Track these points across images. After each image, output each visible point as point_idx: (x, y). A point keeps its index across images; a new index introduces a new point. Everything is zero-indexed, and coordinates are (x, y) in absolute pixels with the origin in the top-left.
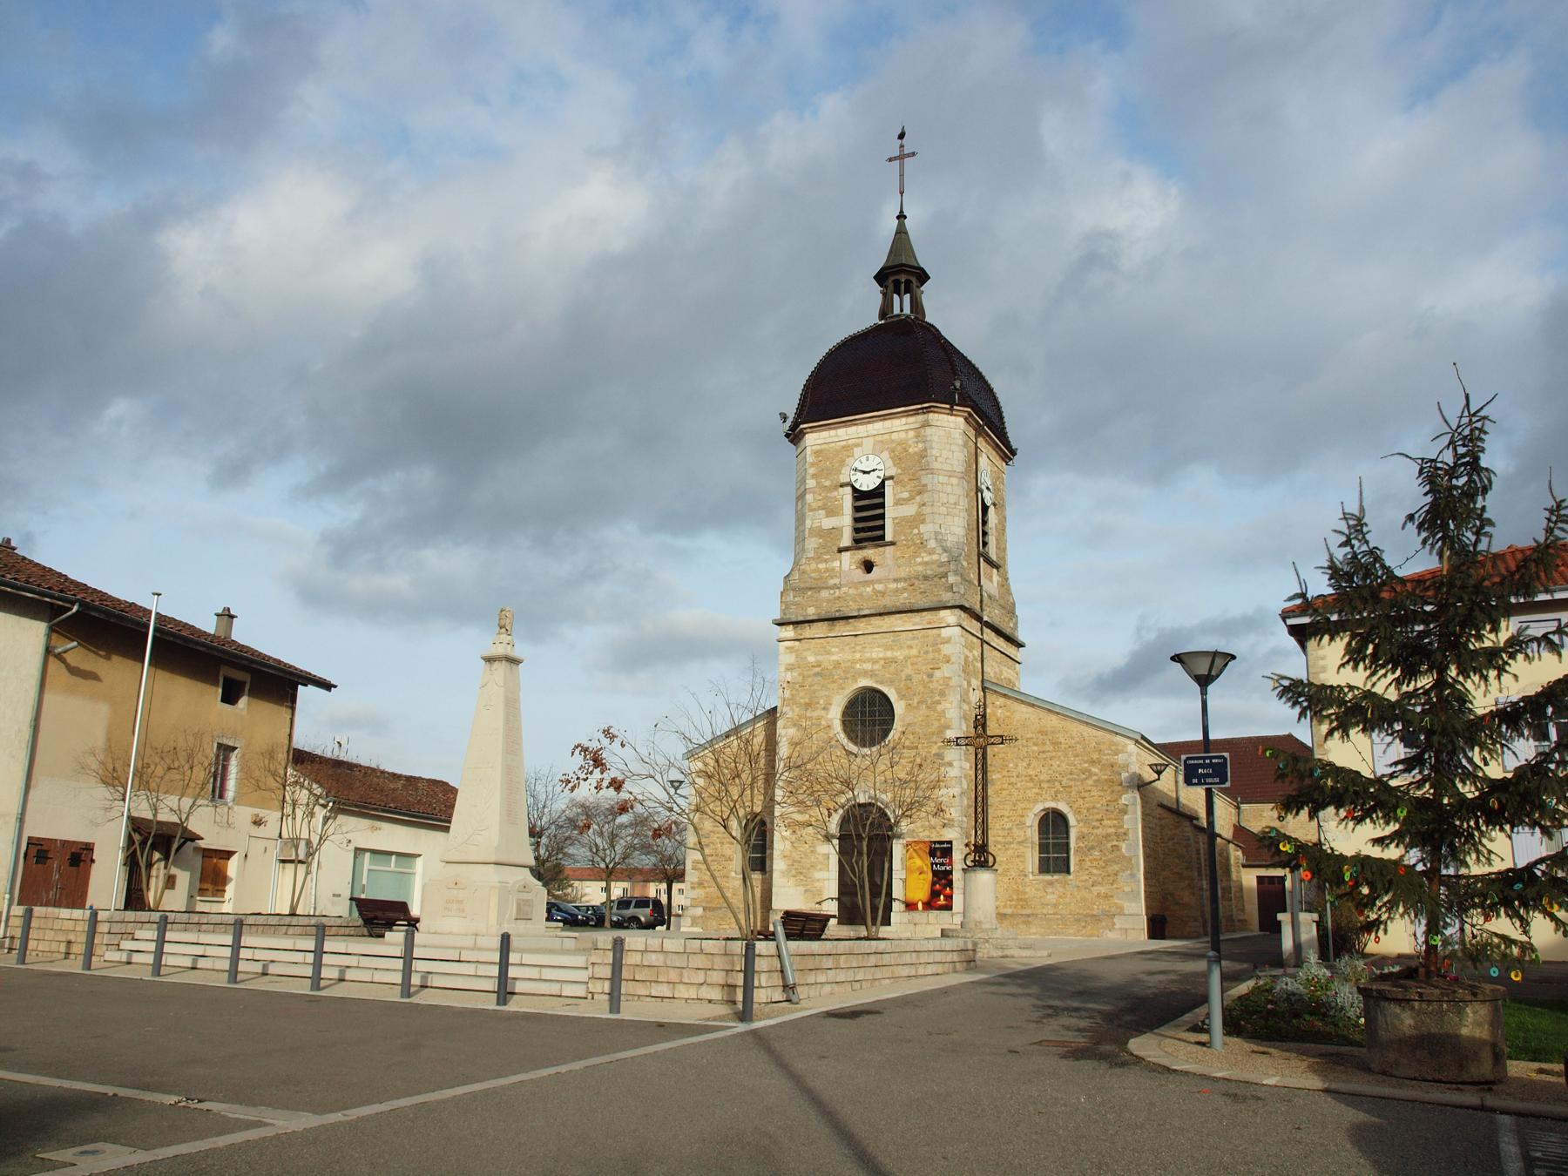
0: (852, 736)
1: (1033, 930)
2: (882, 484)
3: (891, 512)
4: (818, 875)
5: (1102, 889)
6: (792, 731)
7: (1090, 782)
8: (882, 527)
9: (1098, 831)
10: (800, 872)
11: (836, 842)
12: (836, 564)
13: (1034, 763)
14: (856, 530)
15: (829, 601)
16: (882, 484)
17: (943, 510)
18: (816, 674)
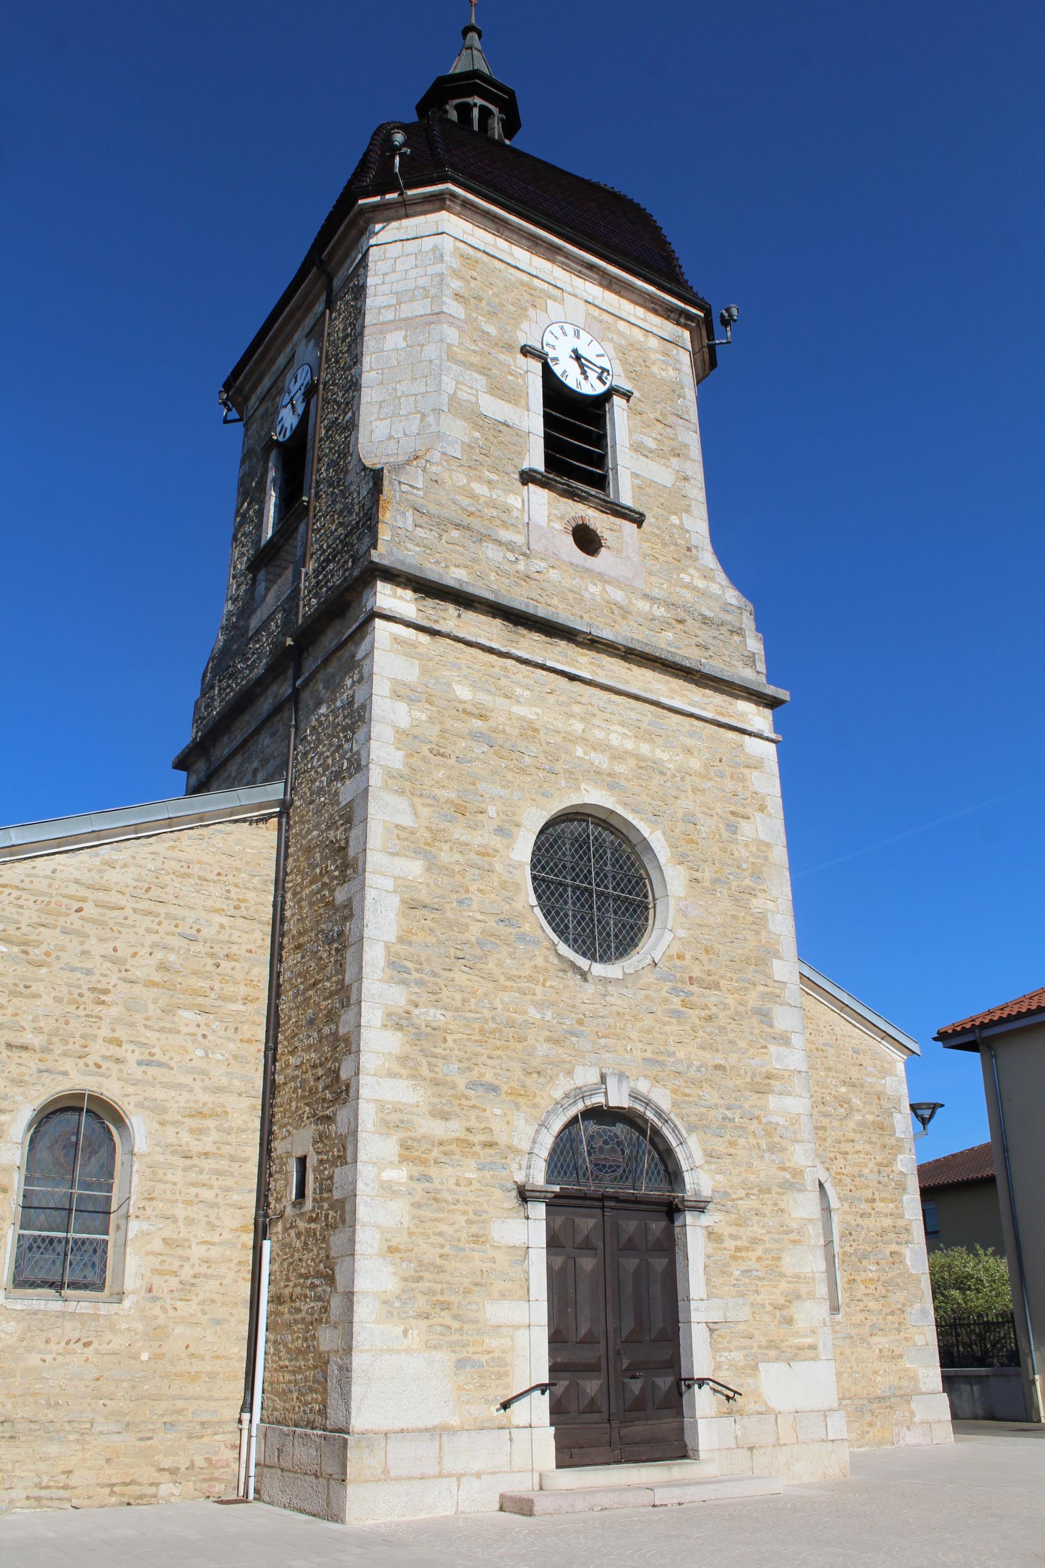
6: (414, 868)
7: (851, 1124)
10: (439, 1301)
11: (539, 1210)
15: (499, 571)
16: (606, 397)
18: (475, 736)
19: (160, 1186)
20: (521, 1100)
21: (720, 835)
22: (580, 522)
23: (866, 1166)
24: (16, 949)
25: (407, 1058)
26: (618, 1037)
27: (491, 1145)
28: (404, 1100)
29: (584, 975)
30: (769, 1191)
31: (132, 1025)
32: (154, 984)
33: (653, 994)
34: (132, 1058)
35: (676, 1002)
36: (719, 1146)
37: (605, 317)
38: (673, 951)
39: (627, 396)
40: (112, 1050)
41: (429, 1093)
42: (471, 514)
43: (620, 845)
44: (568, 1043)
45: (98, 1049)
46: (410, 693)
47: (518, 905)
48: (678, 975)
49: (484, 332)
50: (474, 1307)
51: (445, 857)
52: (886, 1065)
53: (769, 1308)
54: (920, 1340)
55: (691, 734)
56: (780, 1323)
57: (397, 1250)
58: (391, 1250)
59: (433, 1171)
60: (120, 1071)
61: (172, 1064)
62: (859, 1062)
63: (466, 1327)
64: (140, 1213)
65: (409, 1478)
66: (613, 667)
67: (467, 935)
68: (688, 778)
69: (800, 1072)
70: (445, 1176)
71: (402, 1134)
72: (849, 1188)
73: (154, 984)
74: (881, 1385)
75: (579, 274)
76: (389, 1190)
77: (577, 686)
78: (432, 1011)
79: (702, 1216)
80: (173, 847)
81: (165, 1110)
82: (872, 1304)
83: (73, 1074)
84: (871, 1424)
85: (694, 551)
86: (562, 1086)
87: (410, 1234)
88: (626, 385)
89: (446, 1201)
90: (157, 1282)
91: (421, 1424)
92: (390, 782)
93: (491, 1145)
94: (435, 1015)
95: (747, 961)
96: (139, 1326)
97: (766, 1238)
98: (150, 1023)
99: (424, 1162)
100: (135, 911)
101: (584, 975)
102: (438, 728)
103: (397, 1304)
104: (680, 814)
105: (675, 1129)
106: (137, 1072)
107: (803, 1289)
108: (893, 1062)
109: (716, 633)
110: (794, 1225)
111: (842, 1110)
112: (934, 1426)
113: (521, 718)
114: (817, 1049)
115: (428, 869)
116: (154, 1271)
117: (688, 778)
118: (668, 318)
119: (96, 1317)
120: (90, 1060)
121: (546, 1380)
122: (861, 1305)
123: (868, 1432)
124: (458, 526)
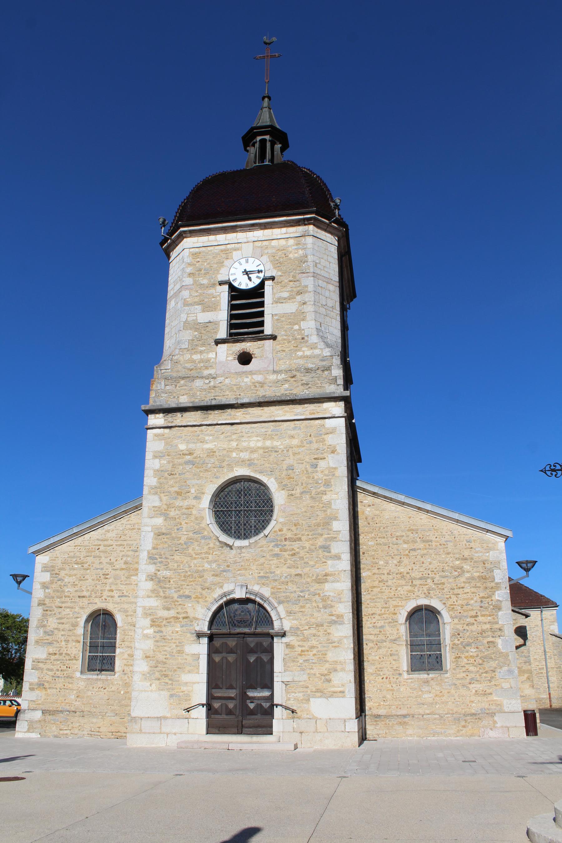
0: (225, 527)
1: (410, 731)
2: (262, 285)
3: (270, 309)
4: (185, 678)
5: (479, 687)
6: (159, 521)
8: (262, 324)
9: (474, 628)
11: (205, 640)
12: (212, 355)
13: (406, 561)
14: (232, 326)
15: (201, 390)
16: (262, 285)
17: (322, 310)
18: (187, 463)
19: (127, 637)
20: (200, 600)
21: (307, 471)
22: (242, 352)
23: (472, 599)
24: (80, 566)
25: (155, 590)
26: (246, 569)
27: (186, 618)
28: (153, 605)
29: (231, 547)
30: (322, 625)
31: (117, 584)
32: (123, 569)
33: (265, 549)
34: (116, 595)
35: (277, 550)
36: (296, 608)
37: (265, 243)
38: (277, 529)
39: (273, 278)
40: (111, 594)
41: (163, 601)
42: (191, 370)
43: (260, 487)
44: (222, 575)
45: (106, 594)
46: (160, 454)
47: (203, 525)
48: (279, 539)
49: (202, 284)
50: (177, 676)
51: (172, 513)
52: (490, 545)
53: (318, 675)
54: (506, 685)
55: (294, 429)
56: (324, 681)
57: (149, 657)
58: (147, 657)
59: (163, 629)
60: (113, 600)
61: (130, 595)
62: (470, 547)
63: (174, 683)
64: (120, 646)
65: (149, 733)
66: (254, 412)
67: (180, 541)
68: (290, 450)
69: (345, 571)
70: (168, 631)
71: (152, 617)
72: (459, 612)
73: (123, 569)
74: (475, 708)
75: (250, 231)
76: (146, 637)
77: (235, 427)
78: (165, 572)
79: (284, 639)
80: (129, 520)
81: (128, 611)
82: (472, 668)
83: (98, 603)
84: (464, 727)
85: (306, 338)
86: (218, 592)
87: (154, 651)
88: (273, 273)
89: (169, 640)
90: (126, 668)
91: (156, 716)
92: (152, 491)
93: (186, 618)
94: (167, 573)
95: (318, 525)
96: (121, 683)
97: (319, 646)
98: (122, 582)
99: (159, 626)
100: (116, 545)
101: (231, 547)
102: (171, 464)
103: (148, 675)
104: (285, 467)
105: (270, 603)
106: (118, 600)
107: (339, 667)
108: (496, 543)
109: (314, 375)
110: (336, 640)
111: (456, 573)
112: (511, 729)
113: (207, 449)
114: (440, 545)
115: (165, 520)
116: (125, 665)
117: (290, 450)
118: (299, 225)
119: (107, 680)
120: (103, 598)
121: (204, 702)
122: (464, 669)
123: (462, 730)
124: (183, 378)
